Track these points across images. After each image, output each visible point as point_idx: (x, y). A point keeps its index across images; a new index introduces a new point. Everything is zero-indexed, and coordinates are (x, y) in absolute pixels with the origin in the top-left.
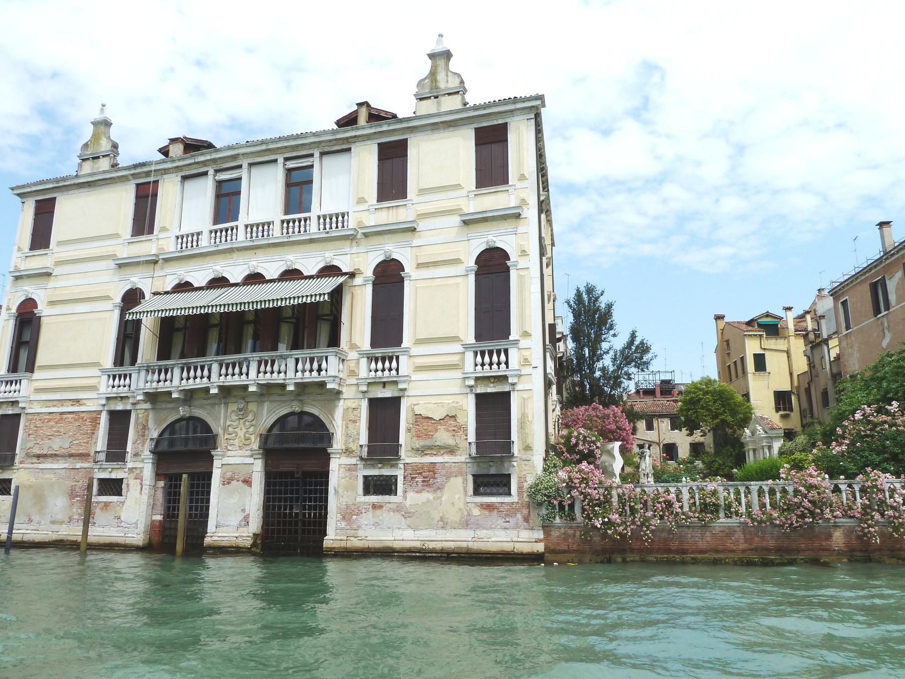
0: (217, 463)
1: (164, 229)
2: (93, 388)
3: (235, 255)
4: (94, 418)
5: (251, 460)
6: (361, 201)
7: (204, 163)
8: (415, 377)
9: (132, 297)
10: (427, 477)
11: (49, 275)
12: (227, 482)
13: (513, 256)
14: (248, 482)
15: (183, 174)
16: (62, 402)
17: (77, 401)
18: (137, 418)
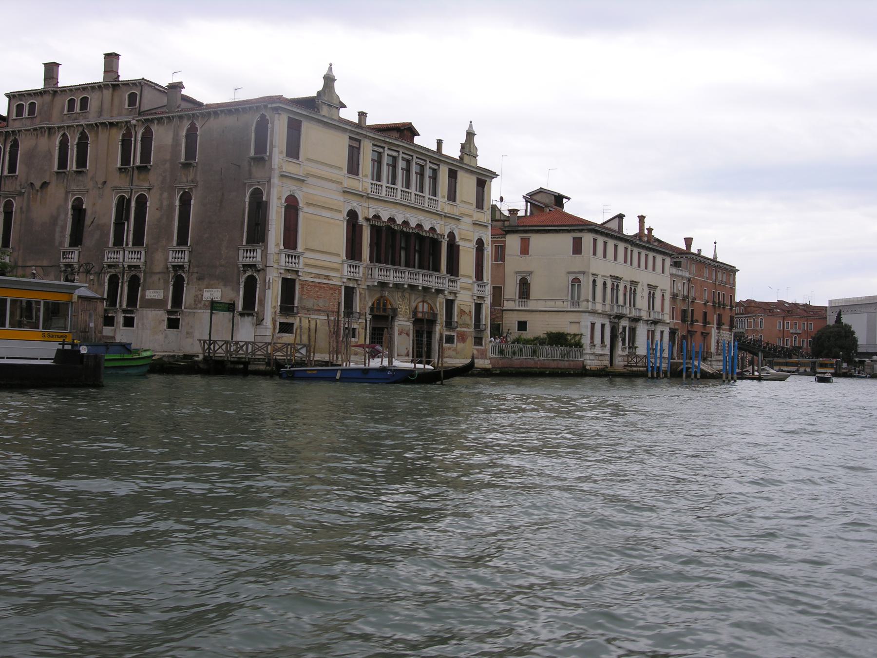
0: (396, 323)
1: (366, 176)
2: (336, 270)
3: (398, 206)
4: (336, 288)
5: (408, 323)
6: (443, 197)
7: (385, 142)
8: (462, 292)
9: (352, 215)
10: (462, 338)
11: (303, 181)
12: (400, 334)
13: (485, 246)
14: (408, 335)
15: (376, 143)
16: (318, 276)
17: (327, 277)
18: (360, 294)
